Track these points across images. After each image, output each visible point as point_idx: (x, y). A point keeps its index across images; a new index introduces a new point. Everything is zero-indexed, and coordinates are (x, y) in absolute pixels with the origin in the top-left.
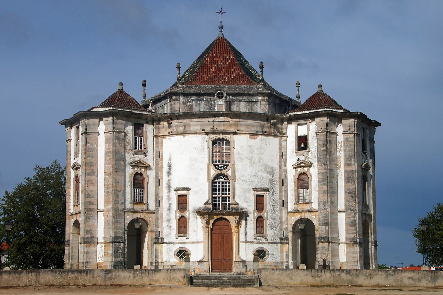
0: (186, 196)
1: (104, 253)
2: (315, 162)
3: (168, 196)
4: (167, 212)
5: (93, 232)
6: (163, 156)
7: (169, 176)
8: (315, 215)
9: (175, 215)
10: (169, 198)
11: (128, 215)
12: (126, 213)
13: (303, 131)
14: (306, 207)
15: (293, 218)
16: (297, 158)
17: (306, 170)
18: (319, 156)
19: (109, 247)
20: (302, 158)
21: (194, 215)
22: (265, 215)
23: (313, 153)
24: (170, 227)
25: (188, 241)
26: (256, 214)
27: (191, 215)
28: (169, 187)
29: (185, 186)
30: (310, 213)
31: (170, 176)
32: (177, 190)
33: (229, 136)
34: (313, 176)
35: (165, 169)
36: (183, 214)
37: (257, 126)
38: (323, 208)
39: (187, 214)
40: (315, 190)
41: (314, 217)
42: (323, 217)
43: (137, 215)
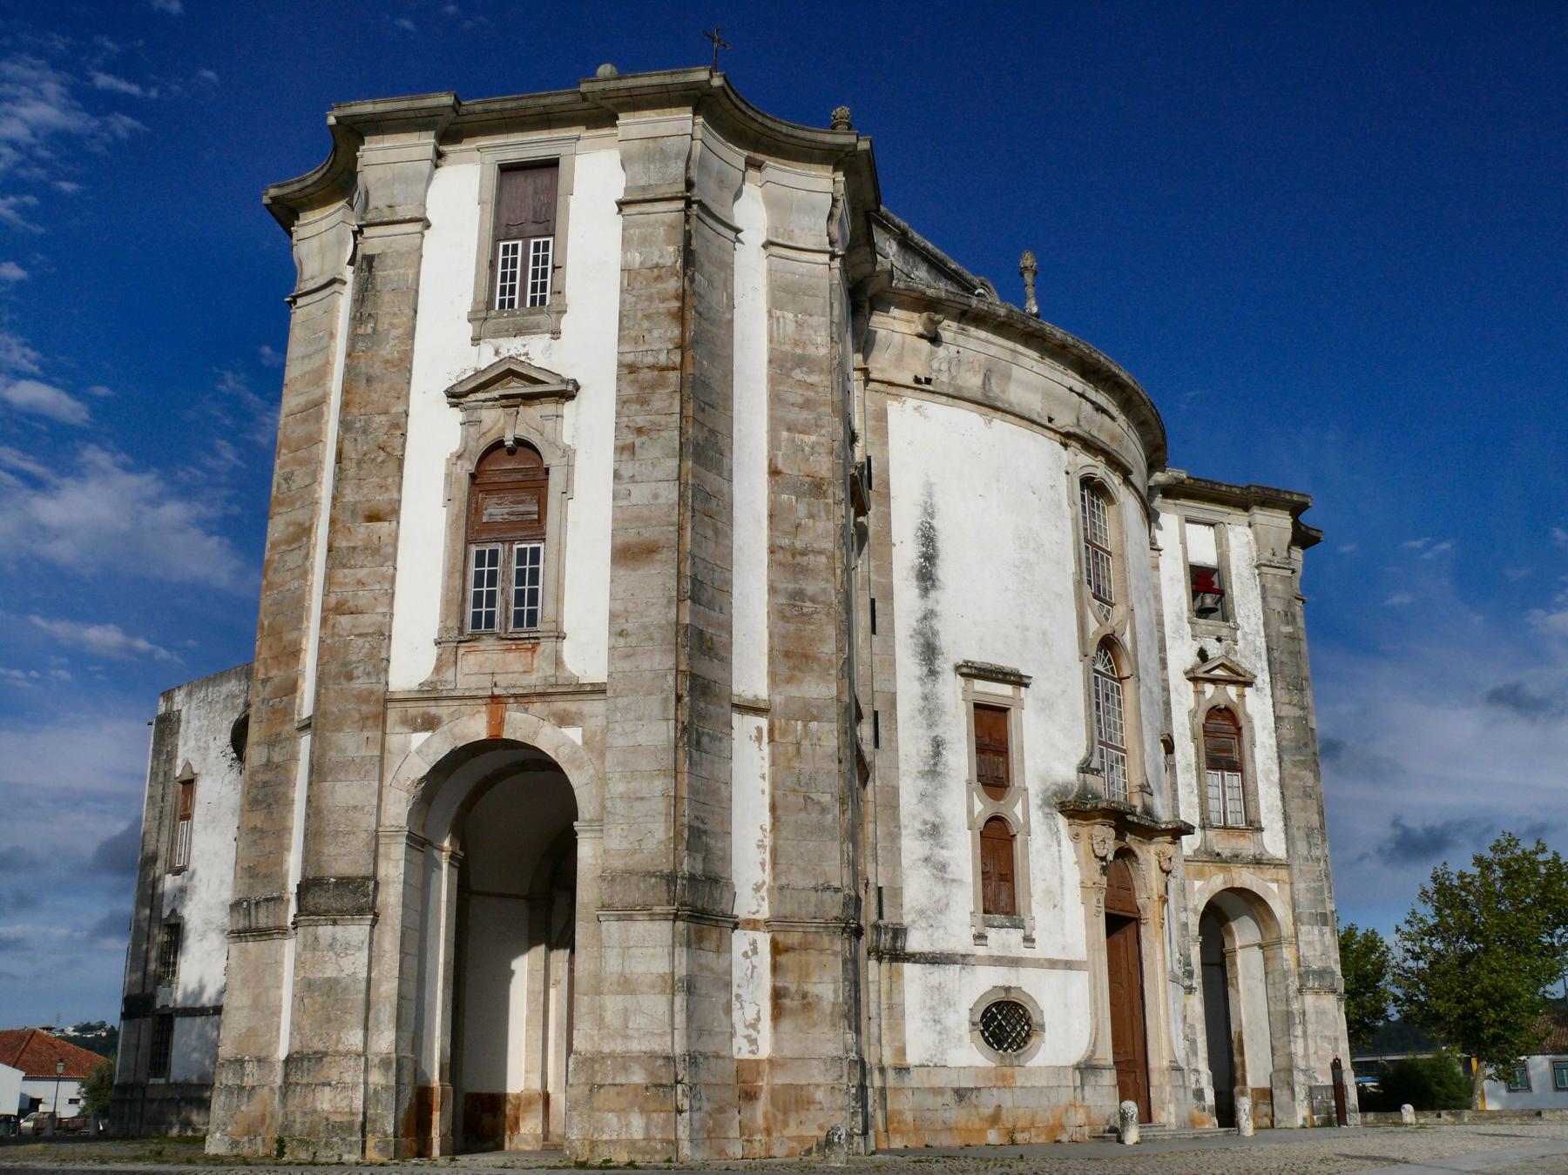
0: (1004, 711)
1: (777, 995)
2: (1263, 678)
3: (925, 698)
4: (922, 784)
5: (712, 842)
6: (887, 485)
7: (925, 592)
8: (1276, 881)
9: (961, 806)
10: (930, 709)
13: (1203, 547)
14: (1246, 846)
15: (1198, 884)
16: (1196, 647)
17: (1235, 698)
18: (1276, 654)
19: (813, 957)
20: (1214, 649)
21: (1046, 815)
23: (1250, 638)
24: (943, 867)
25: (980, 951)
27: (1036, 817)
28: (929, 651)
29: (1008, 663)
30: (1258, 872)
31: (932, 594)
32: (972, 672)
34: (1257, 725)
35: (905, 554)
36: (1000, 808)
38: (1305, 853)
39: (1018, 810)
40: (1268, 780)
41: (1274, 886)
42: (1308, 890)
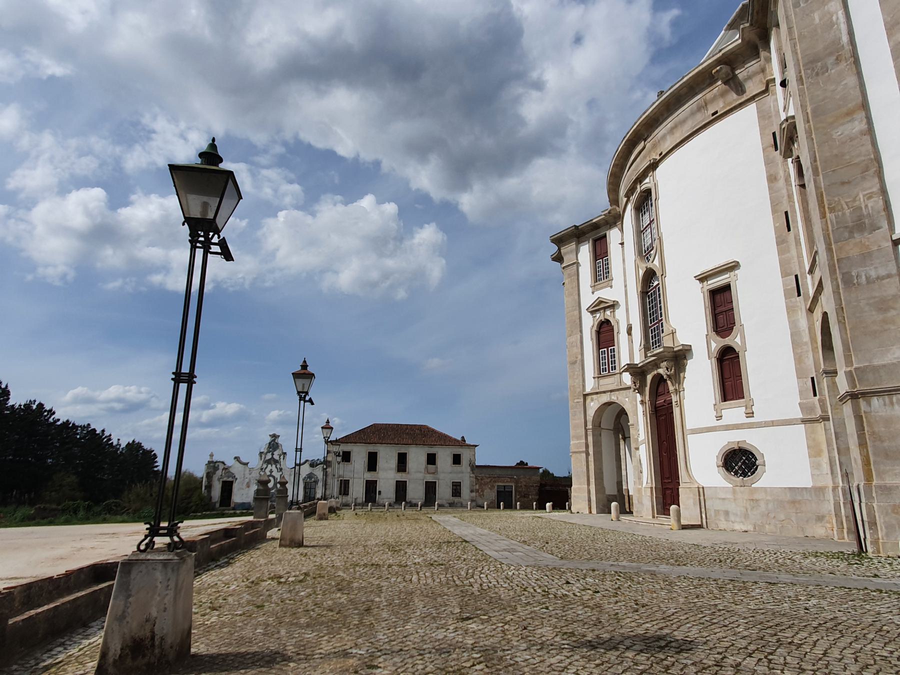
11: (592, 400)
12: (589, 398)
22: (738, 340)
26: (714, 345)
33: (647, 180)
37: (693, 114)
43: (605, 398)
